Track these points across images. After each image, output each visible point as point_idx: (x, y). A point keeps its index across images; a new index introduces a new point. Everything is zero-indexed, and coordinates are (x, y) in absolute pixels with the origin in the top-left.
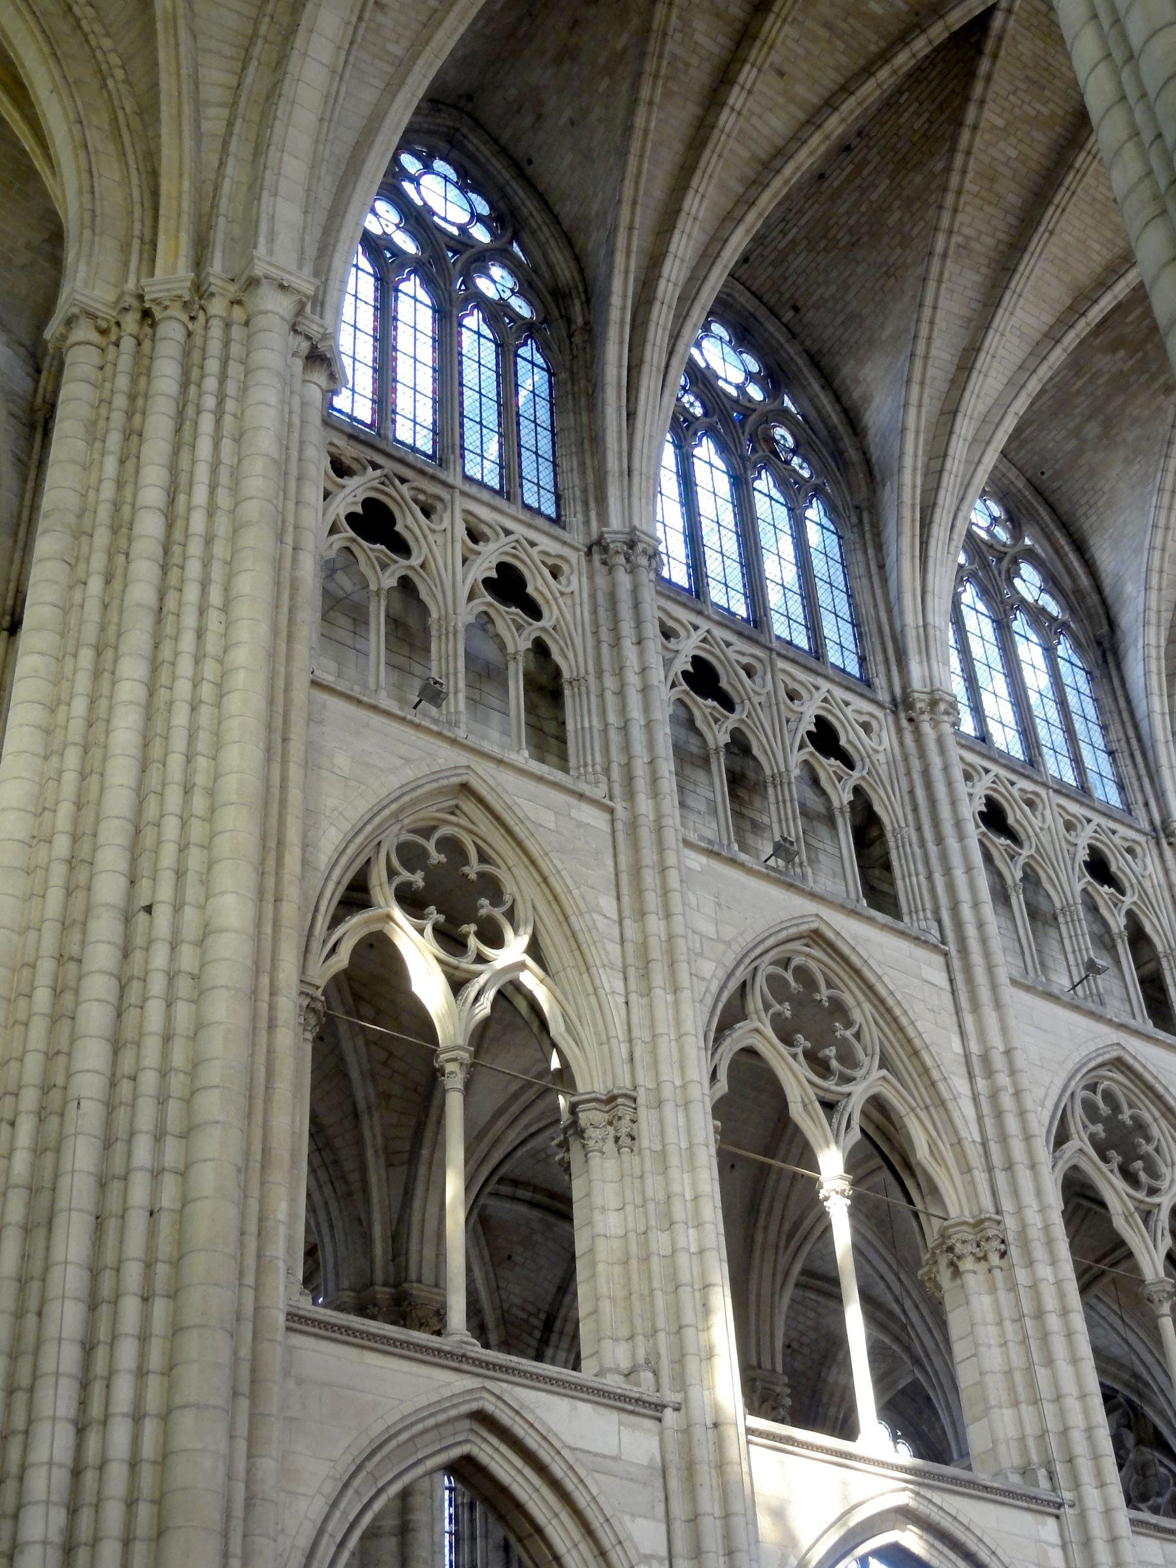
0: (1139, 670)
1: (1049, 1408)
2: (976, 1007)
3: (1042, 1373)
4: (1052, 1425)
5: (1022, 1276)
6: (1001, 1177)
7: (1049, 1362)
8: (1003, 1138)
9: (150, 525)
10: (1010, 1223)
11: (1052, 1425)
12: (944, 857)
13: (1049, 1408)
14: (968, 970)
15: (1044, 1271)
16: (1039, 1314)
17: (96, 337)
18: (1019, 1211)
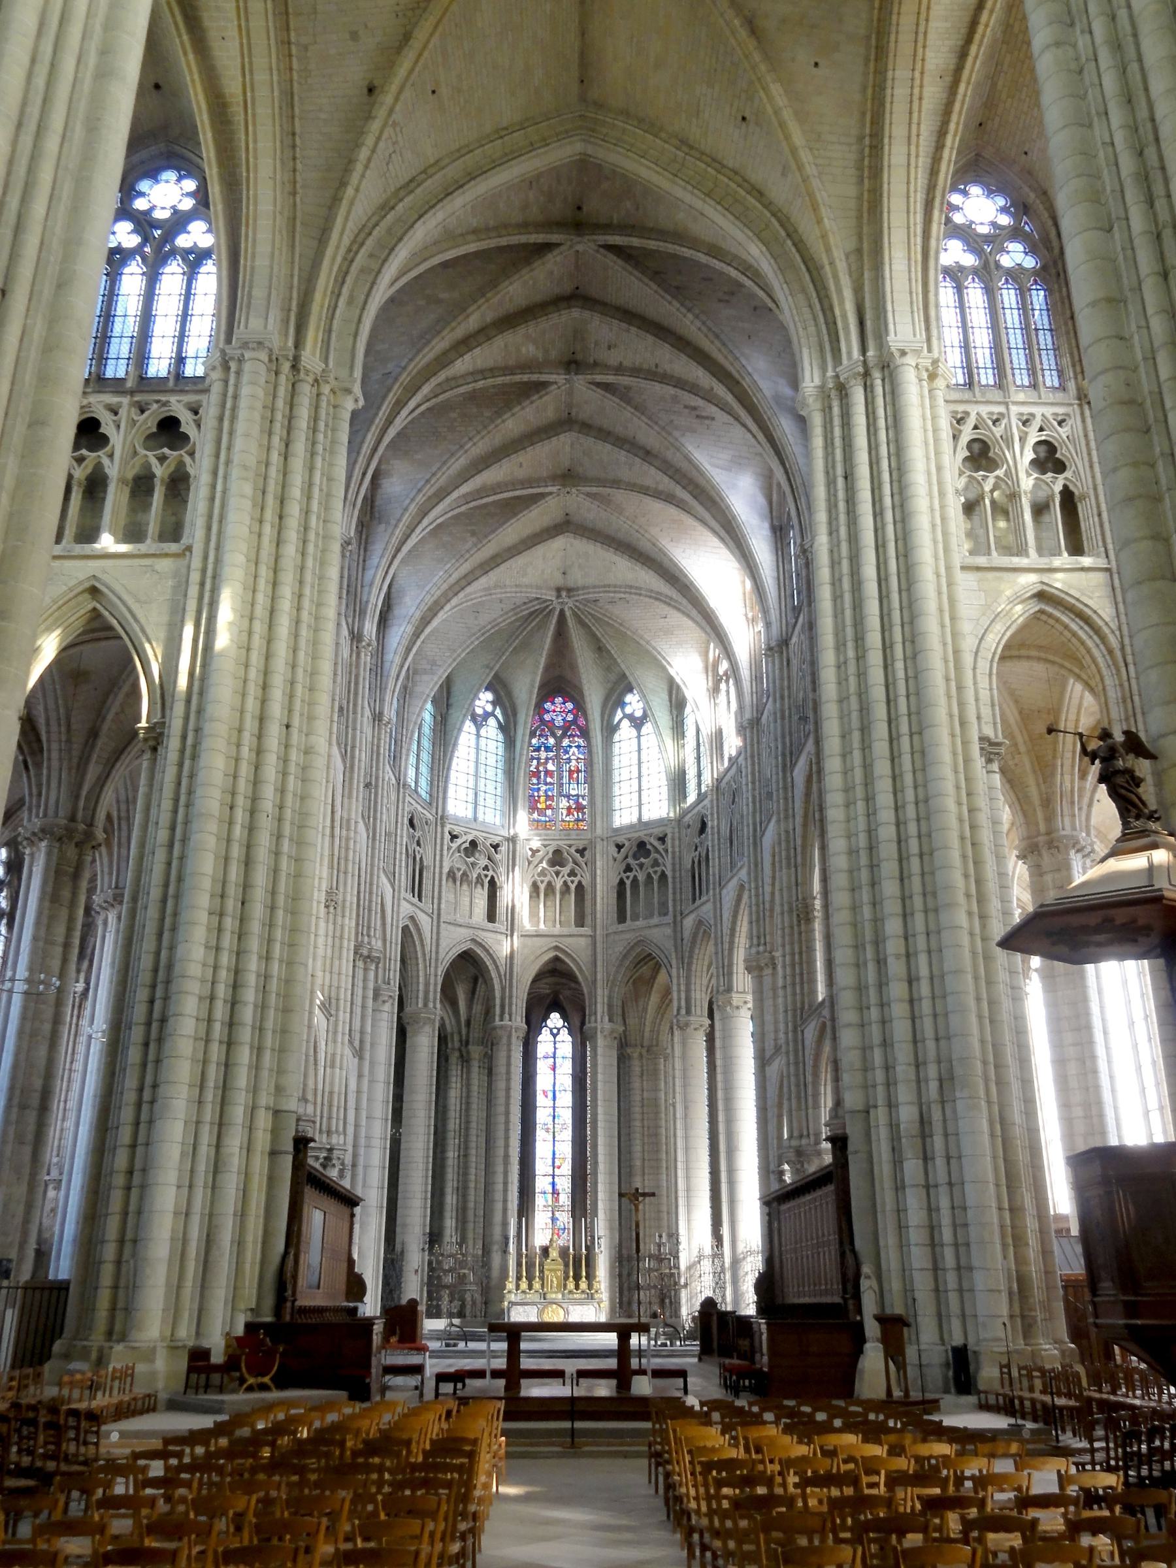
0: (397, 640)
1: (335, 977)
2: (350, 797)
3: (337, 962)
4: (335, 984)
5: (339, 919)
6: (342, 875)
7: (340, 958)
8: (347, 860)
9: (294, 510)
10: (341, 897)
11: (335, 984)
12: (355, 721)
13: (335, 977)
14: (351, 779)
15: (347, 921)
16: (341, 938)
17: (266, 360)
18: (345, 893)
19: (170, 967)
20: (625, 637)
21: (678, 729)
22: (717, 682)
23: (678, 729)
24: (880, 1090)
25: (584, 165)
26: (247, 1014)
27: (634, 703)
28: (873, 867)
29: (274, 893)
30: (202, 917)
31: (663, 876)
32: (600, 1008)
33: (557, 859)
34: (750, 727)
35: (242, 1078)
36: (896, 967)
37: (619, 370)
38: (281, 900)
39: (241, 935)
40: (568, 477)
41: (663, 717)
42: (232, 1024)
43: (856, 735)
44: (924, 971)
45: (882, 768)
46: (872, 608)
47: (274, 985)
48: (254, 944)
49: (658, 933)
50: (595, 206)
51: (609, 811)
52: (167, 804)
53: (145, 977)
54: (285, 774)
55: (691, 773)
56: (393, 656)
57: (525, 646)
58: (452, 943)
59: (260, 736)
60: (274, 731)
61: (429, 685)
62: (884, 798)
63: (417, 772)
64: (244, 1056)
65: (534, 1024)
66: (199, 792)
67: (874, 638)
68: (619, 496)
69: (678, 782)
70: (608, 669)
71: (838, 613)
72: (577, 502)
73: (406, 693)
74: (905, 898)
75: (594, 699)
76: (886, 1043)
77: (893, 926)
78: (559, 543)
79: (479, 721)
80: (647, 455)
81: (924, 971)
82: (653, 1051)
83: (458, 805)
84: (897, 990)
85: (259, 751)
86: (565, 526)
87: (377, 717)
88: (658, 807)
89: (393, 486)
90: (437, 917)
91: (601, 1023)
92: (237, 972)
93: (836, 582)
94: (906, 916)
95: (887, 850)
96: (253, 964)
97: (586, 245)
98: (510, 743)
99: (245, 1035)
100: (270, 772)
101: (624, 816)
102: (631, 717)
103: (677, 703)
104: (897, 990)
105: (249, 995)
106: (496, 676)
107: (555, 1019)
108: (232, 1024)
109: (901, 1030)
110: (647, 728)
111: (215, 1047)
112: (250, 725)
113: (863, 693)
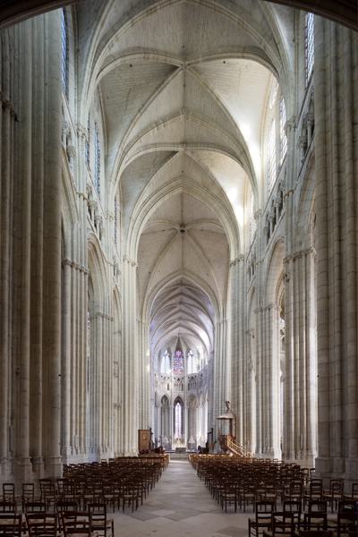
20: (189, 342)
23: (199, 358)
25: (182, 278)
27: (191, 352)
33: (179, 379)
41: (196, 355)
49: (195, 392)
50: (184, 281)
58: (161, 394)
63: (156, 367)
65: (175, 405)
69: (199, 368)
72: (181, 322)
75: (184, 351)
78: (179, 328)
82: (194, 410)
83: (162, 371)
88: (195, 371)
91: (186, 406)
97: (183, 288)
101: (189, 372)
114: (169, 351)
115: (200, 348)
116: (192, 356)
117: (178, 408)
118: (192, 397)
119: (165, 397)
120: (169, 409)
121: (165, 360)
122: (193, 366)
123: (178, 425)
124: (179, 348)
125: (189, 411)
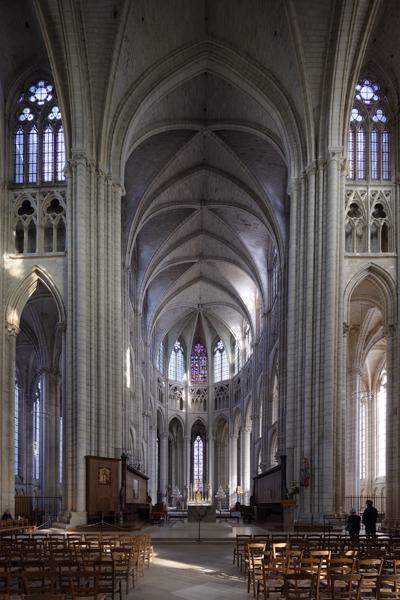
19: (76, 402)
21: (233, 351)
22: (246, 334)
23: (233, 351)
24: (298, 442)
26: (103, 418)
27: (220, 345)
28: (303, 369)
29: (108, 380)
30: (84, 385)
31: (227, 397)
32: (210, 433)
33: (199, 392)
34: (255, 346)
35: (103, 438)
36: (307, 402)
37: (219, 202)
38: (111, 383)
39: (99, 393)
40: (201, 256)
41: (229, 348)
42: (98, 421)
43: (300, 323)
44: (317, 403)
45: (309, 333)
46: (311, 271)
47: (111, 409)
48: (103, 396)
49: (226, 413)
51: (213, 378)
52: (69, 348)
53: (70, 406)
54: (108, 338)
55: (236, 366)
56: (149, 324)
57: (189, 326)
58: (171, 415)
59: (98, 324)
60: (103, 321)
61: (162, 337)
62: (309, 344)
64: (103, 431)
66: (79, 342)
67: (310, 284)
68: (219, 264)
69: (232, 368)
70: (213, 334)
71: (297, 276)
73: (155, 339)
74: (313, 379)
75: (209, 343)
76: (302, 427)
77: (308, 389)
79: (176, 351)
80: (227, 243)
81: (317, 403)
83: (171, 377)
84: (307, 410)
85: (98, 330)
86: (200, 278)
87: (146, 344)
88: (226, 377)
89: (145, 255)
90: (166, 407)
91: (211, 437)
92: (98, 405)
93: (297, 263)
94: (312, 385)
95: (308, 363)
96: (103, 403)
98: (185, 358)
99: (103, 424)
100: (103, 337)
101: (217, 380)
102: (219, 350)
103: (233, 343)
104: (307, 410)
105: (103, 412)
106: (180, 337)
107: (198, 438)
108: (98, 421)
109: (307, 422)
110: (224, 353)
111: (93, 428)
112: (94, 319)
113: (304, 307)
114: (183, 344)
115: (236, 329)
116: (221, 351)
117: (198, 445)
118: (222, 423)
119: (176, 422)
120: (182, 442)
121: (176, 359)
122: (223, 368)
123: (198, 469)
124: (199, 340)
125: (216, 447)
